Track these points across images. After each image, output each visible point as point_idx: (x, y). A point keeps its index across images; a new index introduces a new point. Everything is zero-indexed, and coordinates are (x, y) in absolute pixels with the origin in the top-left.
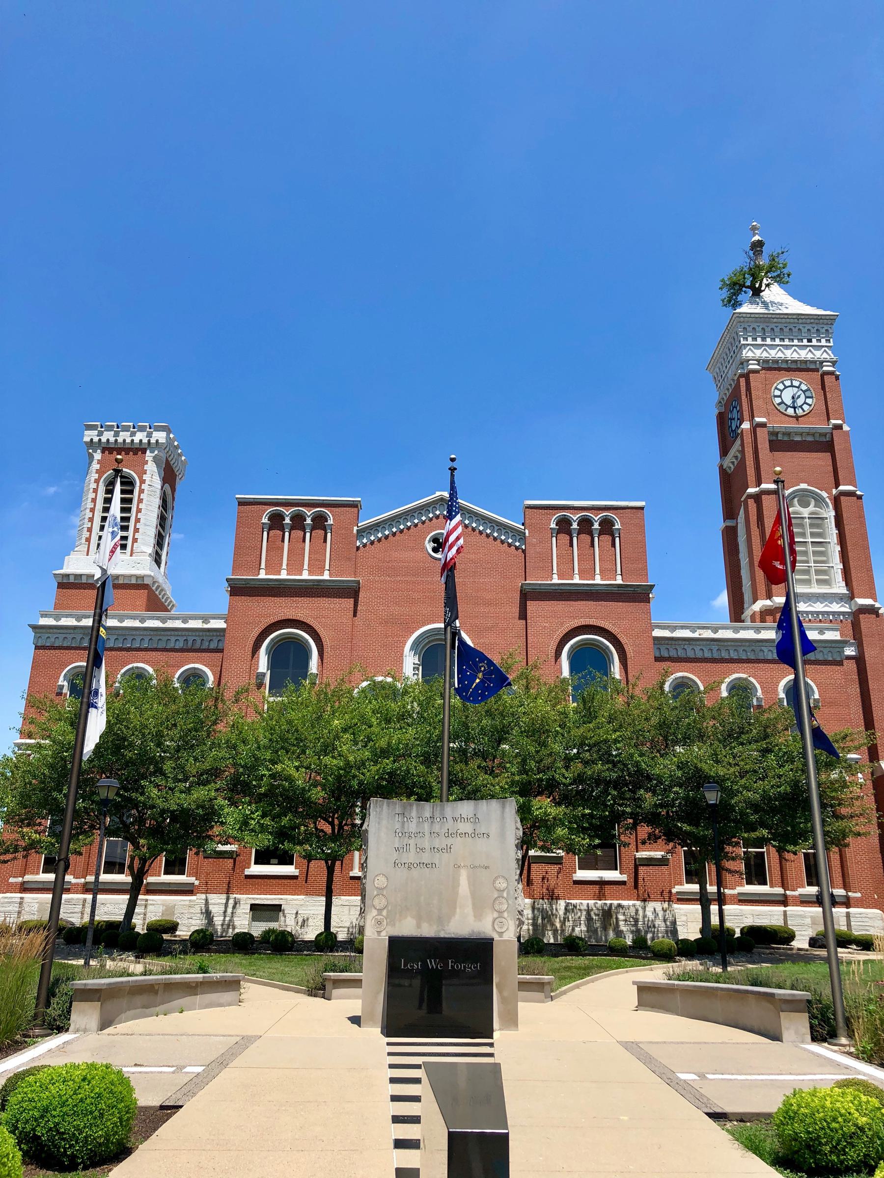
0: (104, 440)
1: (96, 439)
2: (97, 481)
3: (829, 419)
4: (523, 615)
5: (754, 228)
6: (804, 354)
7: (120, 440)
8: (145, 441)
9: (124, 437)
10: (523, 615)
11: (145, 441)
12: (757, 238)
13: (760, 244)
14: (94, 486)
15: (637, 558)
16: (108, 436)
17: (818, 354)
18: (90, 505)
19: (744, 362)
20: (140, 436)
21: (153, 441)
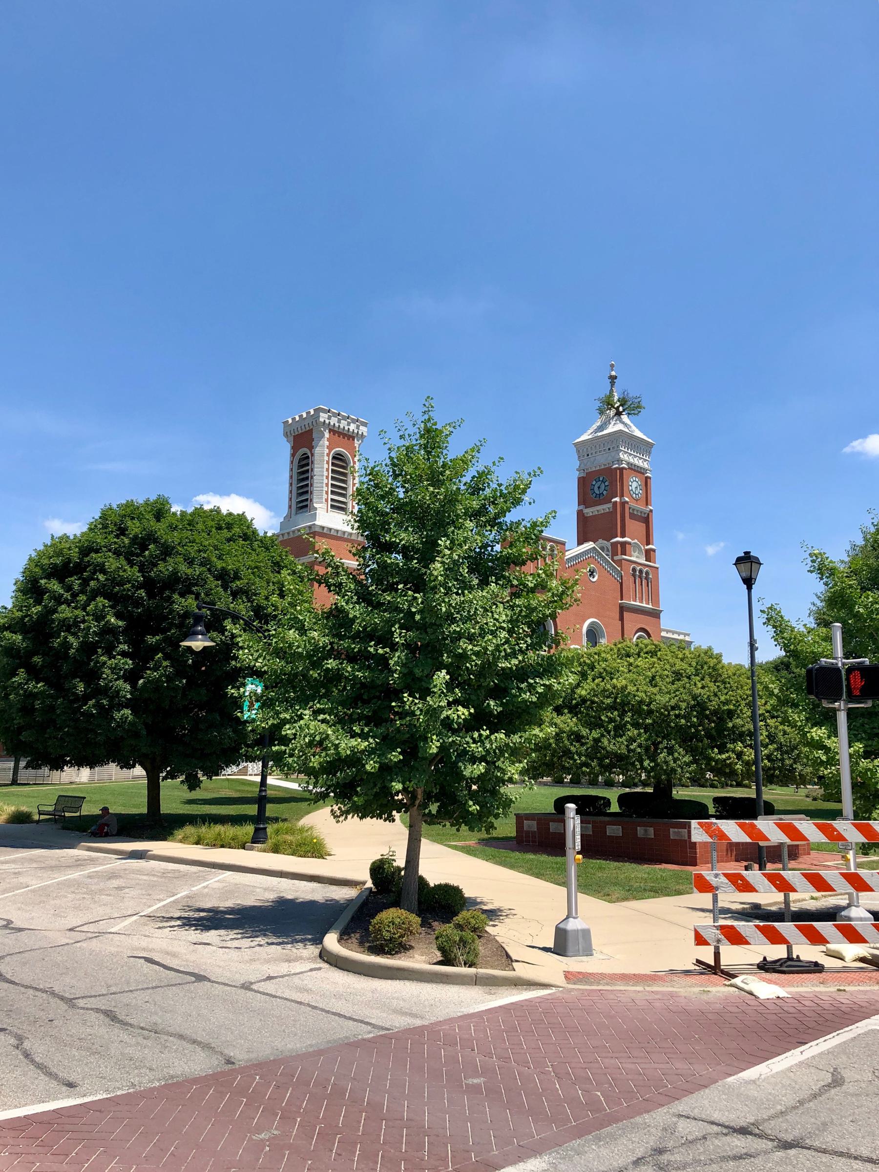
0: (332, 424)
1: (327, 421)
2: (328, 455)
3: (647, 504)
4: (622, 619)
5: (612, 366)
6: (640, 463)
7: (342, 427)
8: (356, 431)
9: (343, 423)
10: (622, 619)
11: (356, 431)
12: (613, 373)
13: (616, 377)
14: (326, 458)
15: (654, 596)
16: (334, 421)
17: (645, 465)
18: (325, 474)
19: (620, 461)
20: (352, 427)
21: (360, 433)
